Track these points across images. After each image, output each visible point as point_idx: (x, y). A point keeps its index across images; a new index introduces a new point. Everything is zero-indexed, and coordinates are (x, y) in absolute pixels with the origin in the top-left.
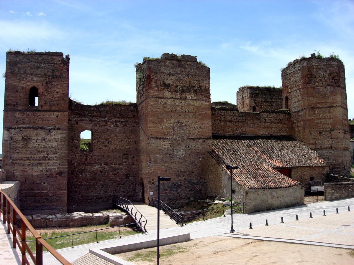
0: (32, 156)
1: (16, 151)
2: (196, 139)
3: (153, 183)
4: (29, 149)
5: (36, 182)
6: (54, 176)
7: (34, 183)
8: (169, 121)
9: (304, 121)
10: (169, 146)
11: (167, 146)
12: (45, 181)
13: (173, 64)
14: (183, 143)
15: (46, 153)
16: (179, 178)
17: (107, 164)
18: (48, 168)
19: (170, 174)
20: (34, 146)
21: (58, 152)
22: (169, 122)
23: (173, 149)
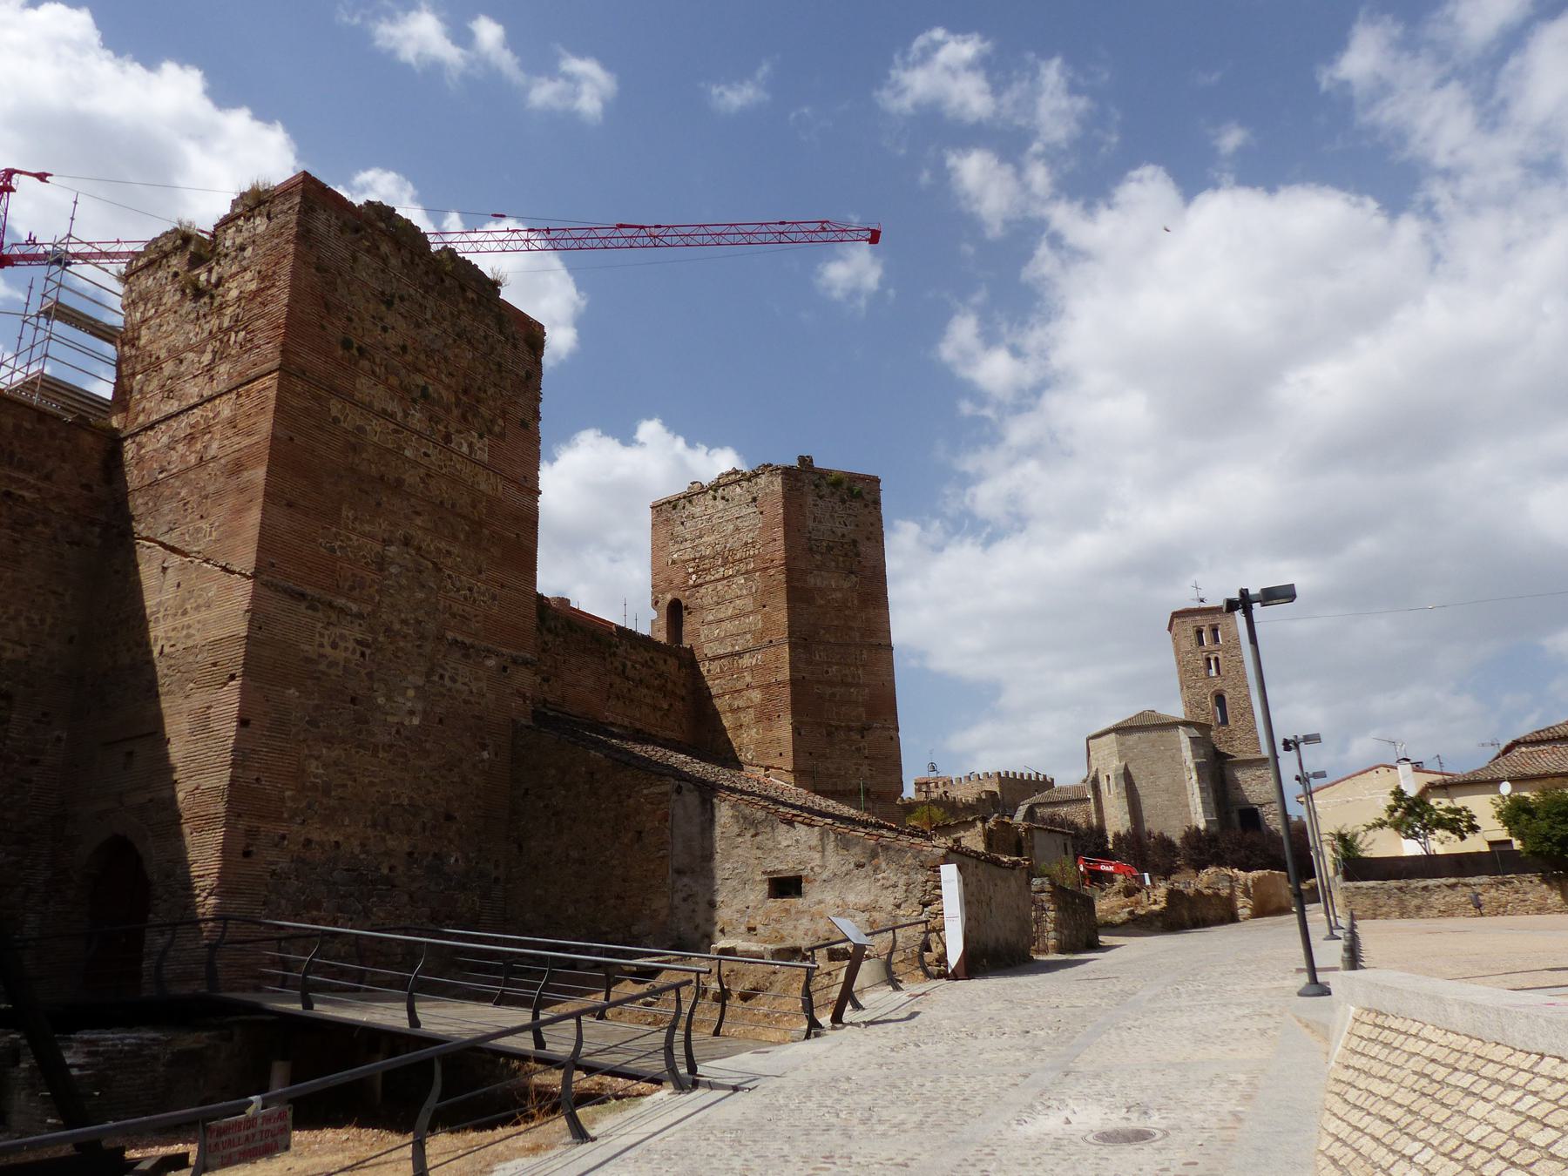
9: (769, 685)
16: (383, 839)
22: (367, 528)
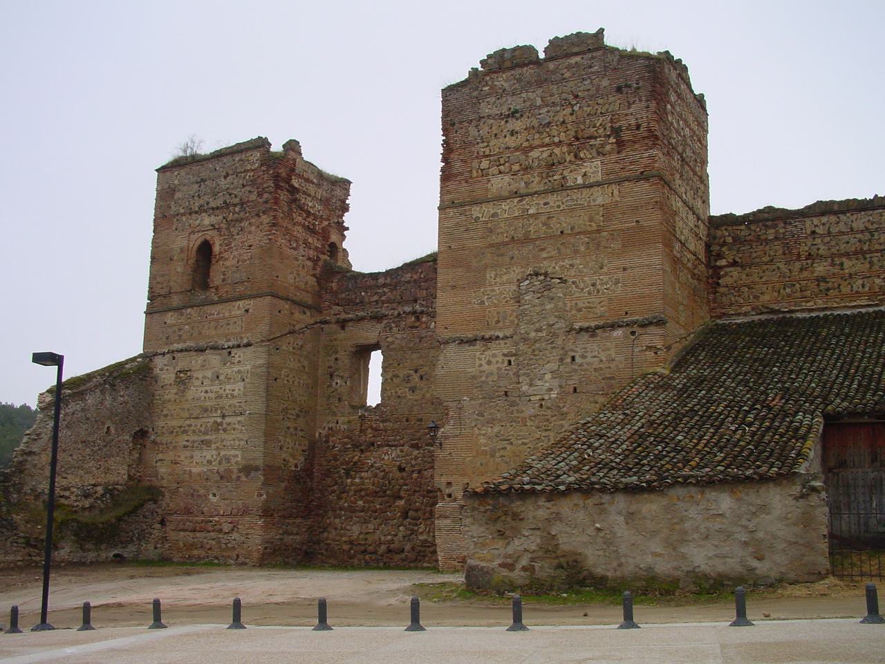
0: (192, 422)
1: (162, 411)
2: (597, 327)
3: (450, 496)
4: (186, 406)
5: (198, 491)
6: (234, 476)
7: (192, 495)
8: (505, 273)
10: (503, 363)
12: (215, 491)
13: (519, 80)
14: (553, 348)
15: (219, 412)
17: (416, 447)
18: (222, 453)
19: (507, 463)
20: (197, 396)
21: (245, 408)
22: (505, 278)
23: (517, 375)
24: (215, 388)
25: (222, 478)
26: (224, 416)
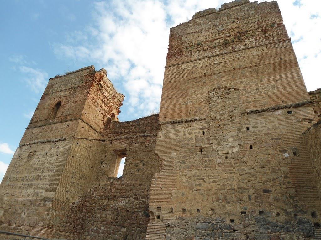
0: (28, 175)
2: (264, 111)
6: (38, 203)
8: (201, 89)
10: (199, 132)
11: (195, 133)
14: (232, 123)
16: (224, 207)
18: (36, 191)
19: (201, 195)
24: (43, 159)
25: (31, 204)
26: (43, 172)
